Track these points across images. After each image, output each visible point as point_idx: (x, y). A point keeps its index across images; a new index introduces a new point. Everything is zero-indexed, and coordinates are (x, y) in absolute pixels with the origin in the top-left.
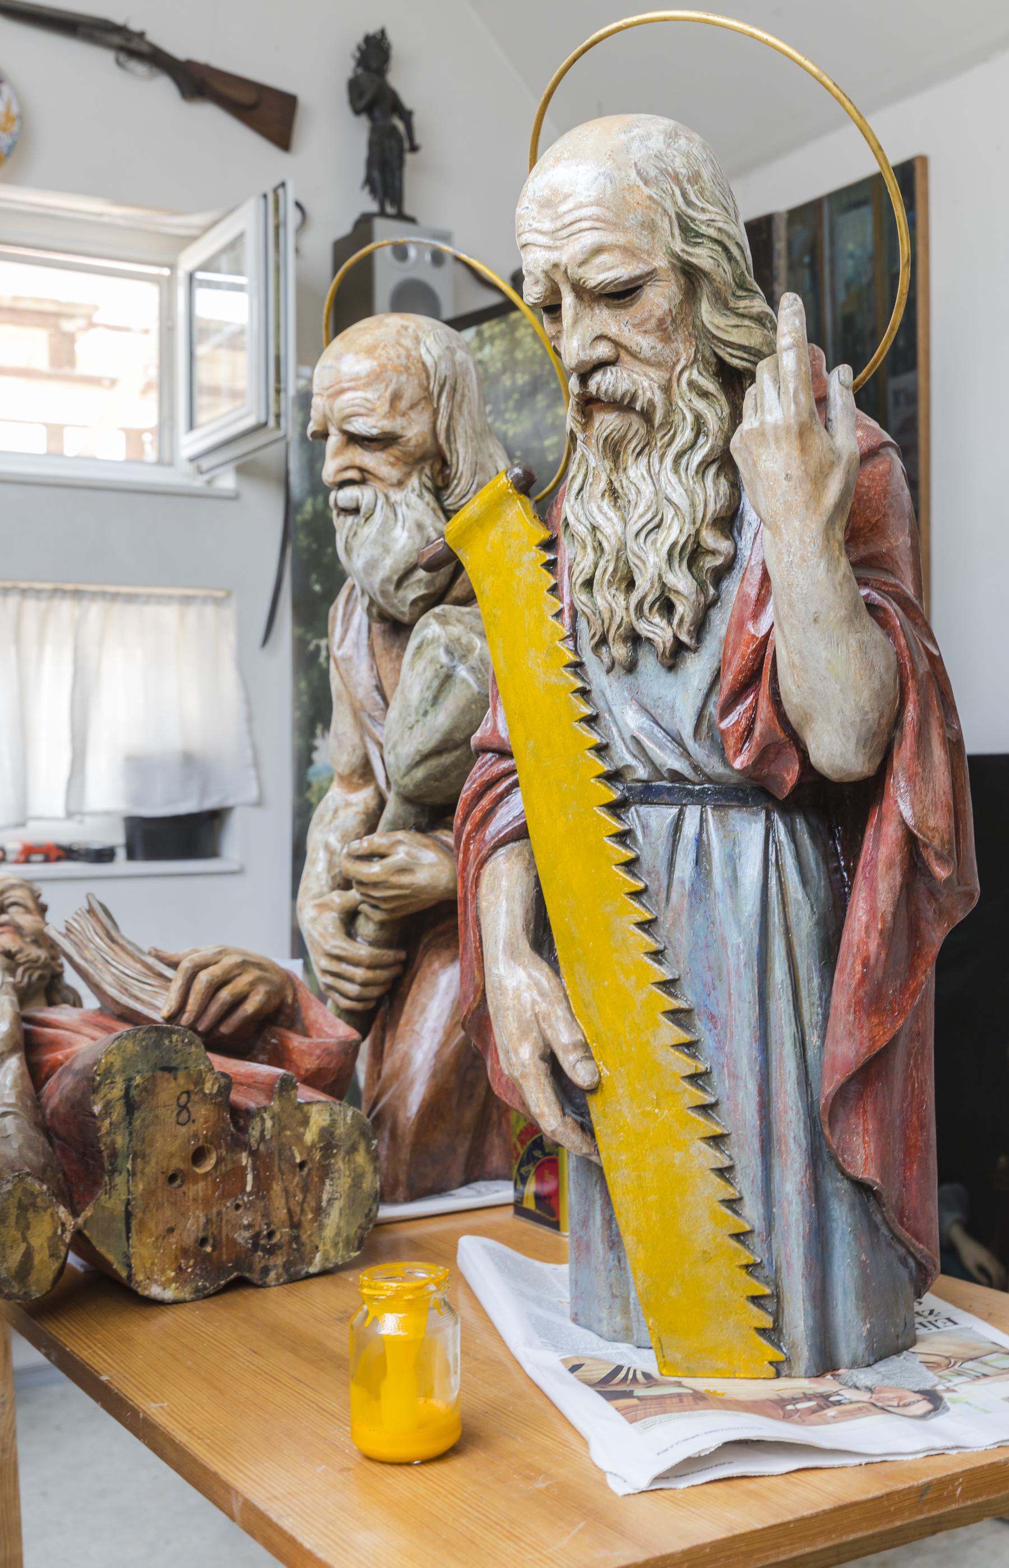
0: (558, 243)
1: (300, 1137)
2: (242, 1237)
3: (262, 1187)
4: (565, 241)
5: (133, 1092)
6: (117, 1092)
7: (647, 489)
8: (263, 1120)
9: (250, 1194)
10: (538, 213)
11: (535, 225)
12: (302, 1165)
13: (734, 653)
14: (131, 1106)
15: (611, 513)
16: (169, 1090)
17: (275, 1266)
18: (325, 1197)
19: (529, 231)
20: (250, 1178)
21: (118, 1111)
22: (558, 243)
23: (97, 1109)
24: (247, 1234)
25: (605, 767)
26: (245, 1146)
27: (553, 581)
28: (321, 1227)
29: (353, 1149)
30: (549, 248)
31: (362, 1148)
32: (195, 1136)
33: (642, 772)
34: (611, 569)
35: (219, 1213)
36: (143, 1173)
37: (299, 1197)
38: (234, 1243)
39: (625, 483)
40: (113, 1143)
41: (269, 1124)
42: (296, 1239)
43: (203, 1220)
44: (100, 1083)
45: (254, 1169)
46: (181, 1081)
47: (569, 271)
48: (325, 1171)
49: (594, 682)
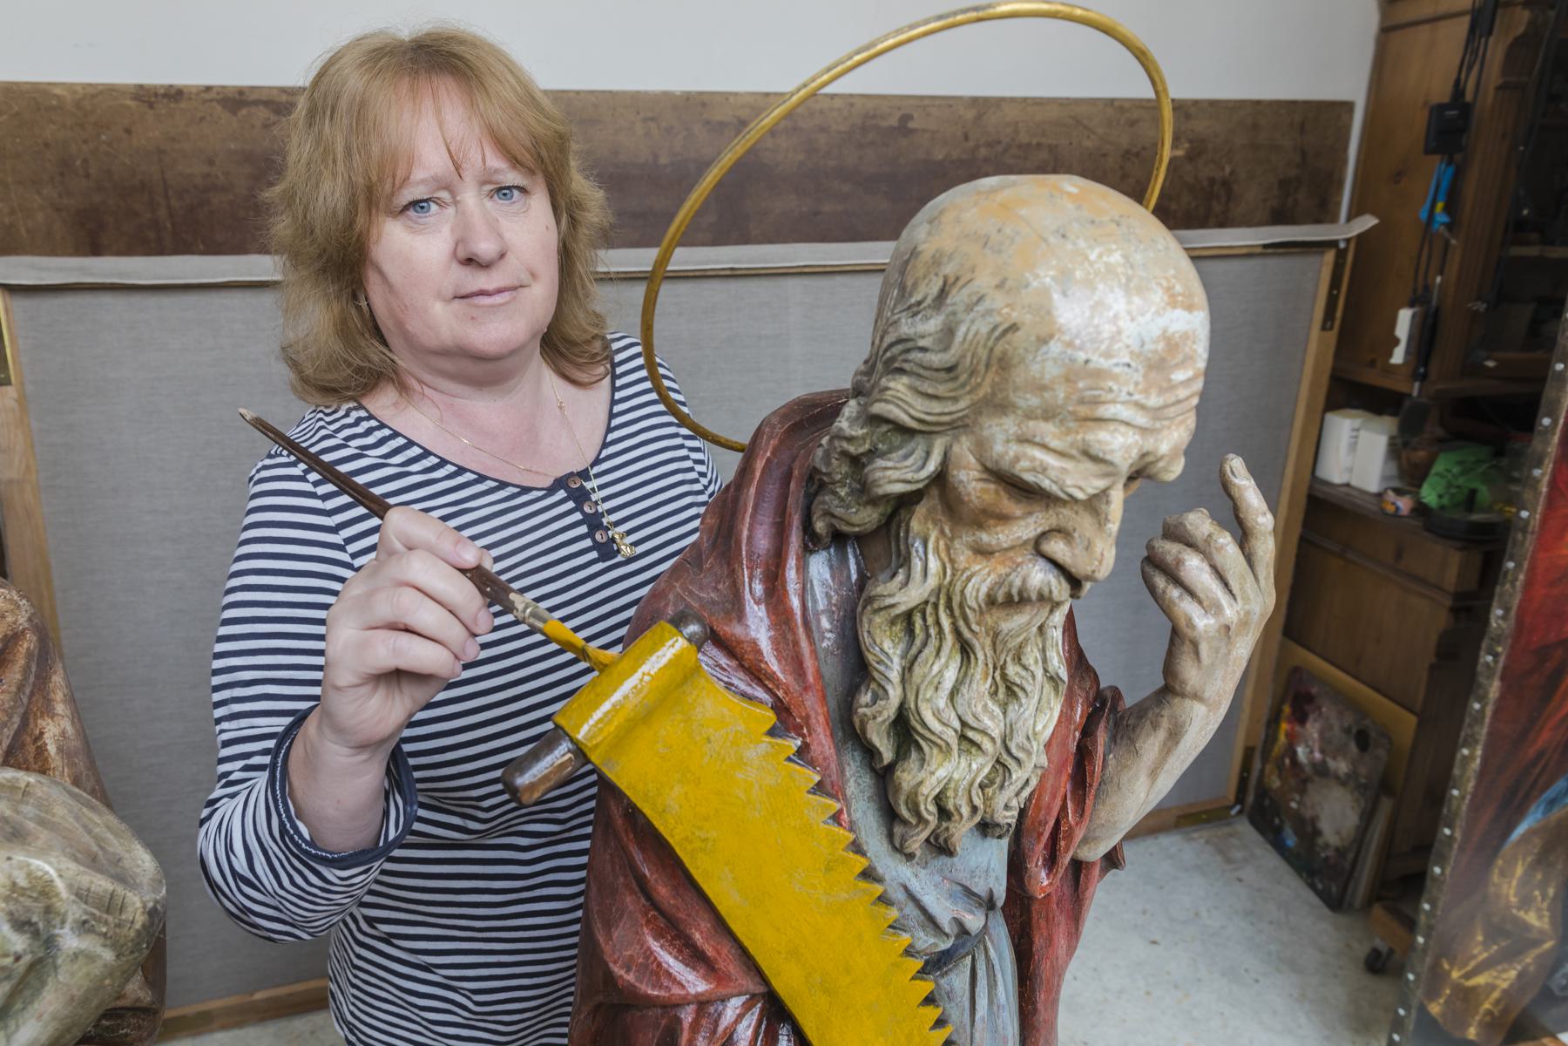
0: (1158, 425)
4: (1166, 423)
7: (1039, 673)
10: (1145, 376)
11: (1136, 397)
13: (1054, 797)
15: (997, 710)
19: (1123, 403)
22: (1158, 425)
25: (918, 964)
27: (817, 778)
30: (1144, 431)
33: (945, 945)
34: (986, 770)
39: (1012, 670)
47: (1161, 464)
49: (887, 877)
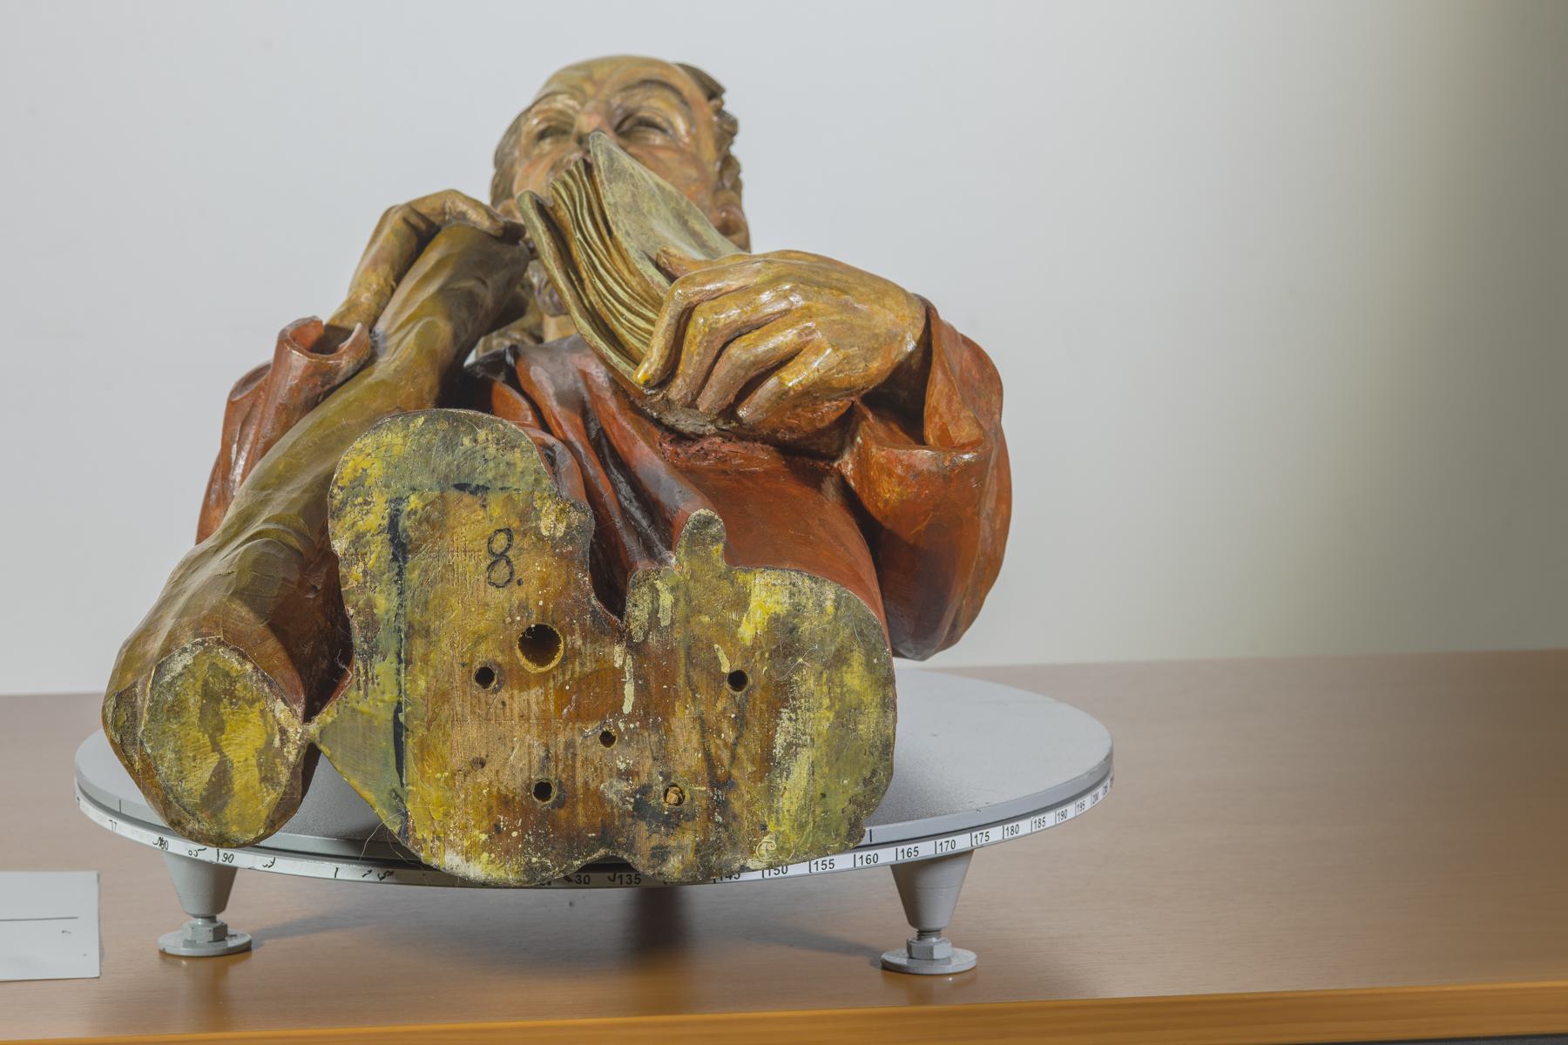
1: (728, 632)
2: (615, 790)
3: (654, 709)
5: (405, 523)
6: (375, 518)
8: (655, 592)
9: (630, 718)
12: (738, 679)
14: (401, 548)
16: (472, 525)
17: (680, 848)
18: (780, 740)
20: (629, 690)
21: (378, 552)
23: (339, 546)
24: (624, 786)
26: (622, 635)
28: (771, 792)
29: (840, 660)
31: (857, 658)
32: (523, 607)
35: (570, 745)
36: (425, 660)
37: (729, 734)
38: (600, 799)
40: (370, 605)
41: (666, 599)
42: (722, 806)
43: (538, 752)
44: (344, 503)
45: (636, 677)
46: (496, 510)
48: (781, 695)
